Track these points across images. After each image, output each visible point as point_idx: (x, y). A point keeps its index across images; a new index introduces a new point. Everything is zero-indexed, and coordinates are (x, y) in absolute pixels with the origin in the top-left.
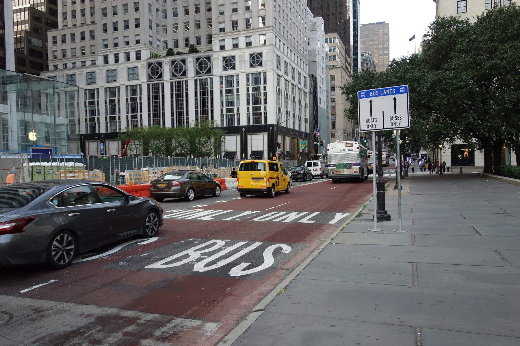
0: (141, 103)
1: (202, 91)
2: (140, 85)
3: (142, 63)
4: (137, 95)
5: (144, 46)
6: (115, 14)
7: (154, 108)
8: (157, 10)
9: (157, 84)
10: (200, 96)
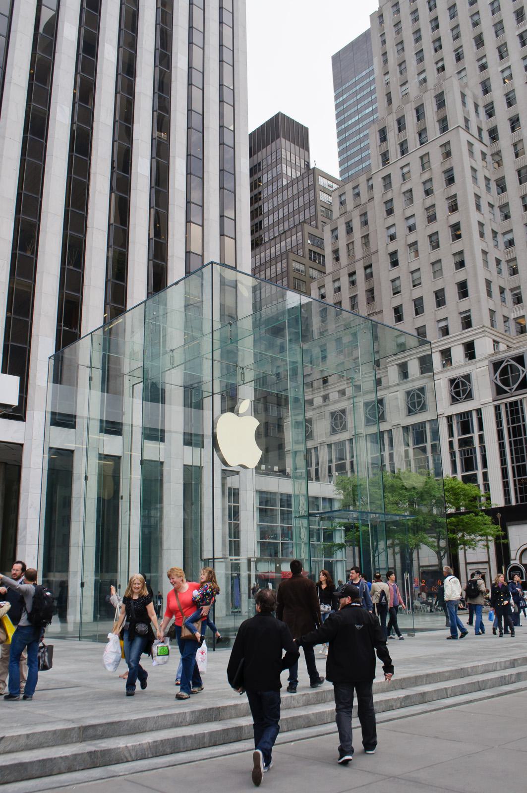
0: (483, 449)
1: (513, 427)
2: (479, 411)
3: (479, 365)
4: (426, 442)
5: (482, 330)
6: (396, 292)
7: (514, 456)
8: (498, 262)
9: (516, 402)
10: (510, 437)
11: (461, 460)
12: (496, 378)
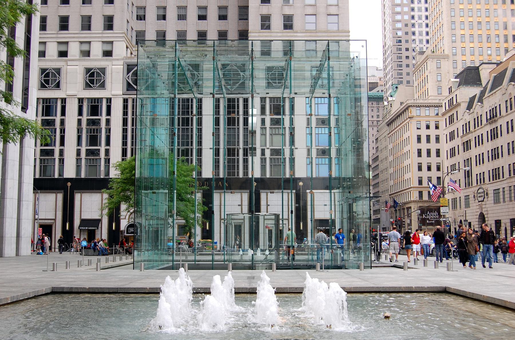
0: (109, 131)
3: (115, 63)
11: (87, 136)
12: (129, 77)
